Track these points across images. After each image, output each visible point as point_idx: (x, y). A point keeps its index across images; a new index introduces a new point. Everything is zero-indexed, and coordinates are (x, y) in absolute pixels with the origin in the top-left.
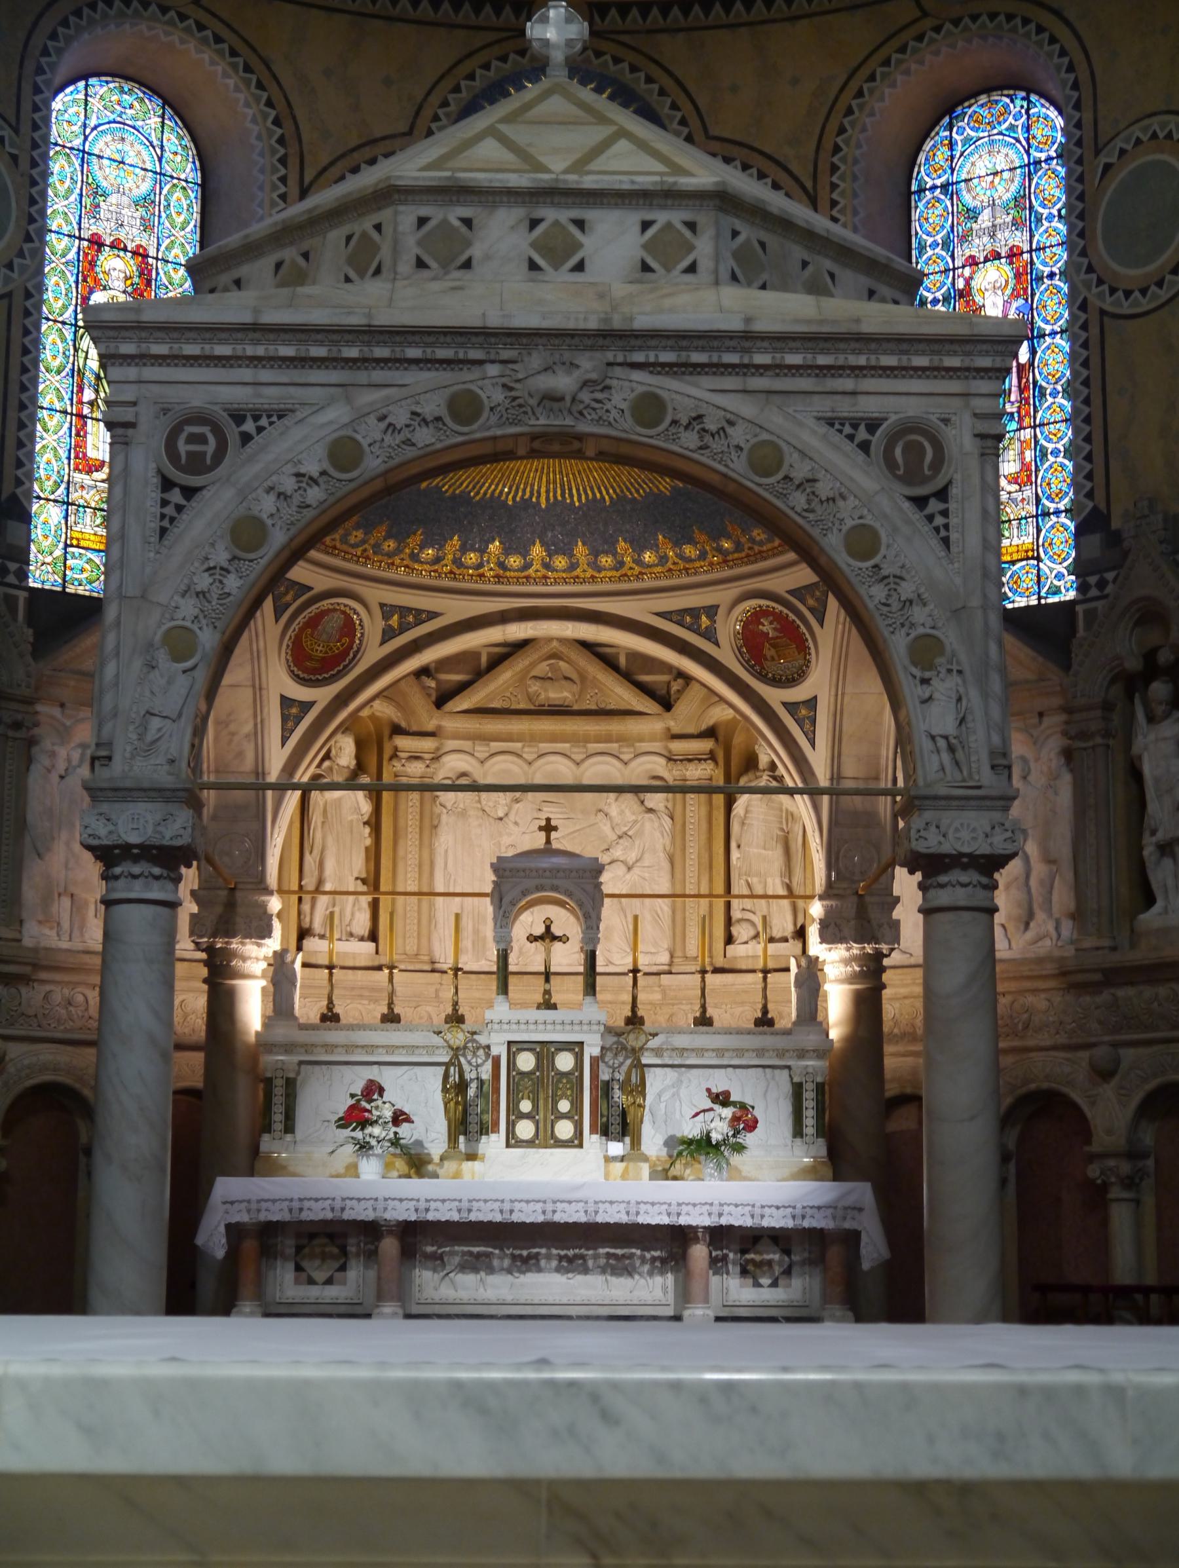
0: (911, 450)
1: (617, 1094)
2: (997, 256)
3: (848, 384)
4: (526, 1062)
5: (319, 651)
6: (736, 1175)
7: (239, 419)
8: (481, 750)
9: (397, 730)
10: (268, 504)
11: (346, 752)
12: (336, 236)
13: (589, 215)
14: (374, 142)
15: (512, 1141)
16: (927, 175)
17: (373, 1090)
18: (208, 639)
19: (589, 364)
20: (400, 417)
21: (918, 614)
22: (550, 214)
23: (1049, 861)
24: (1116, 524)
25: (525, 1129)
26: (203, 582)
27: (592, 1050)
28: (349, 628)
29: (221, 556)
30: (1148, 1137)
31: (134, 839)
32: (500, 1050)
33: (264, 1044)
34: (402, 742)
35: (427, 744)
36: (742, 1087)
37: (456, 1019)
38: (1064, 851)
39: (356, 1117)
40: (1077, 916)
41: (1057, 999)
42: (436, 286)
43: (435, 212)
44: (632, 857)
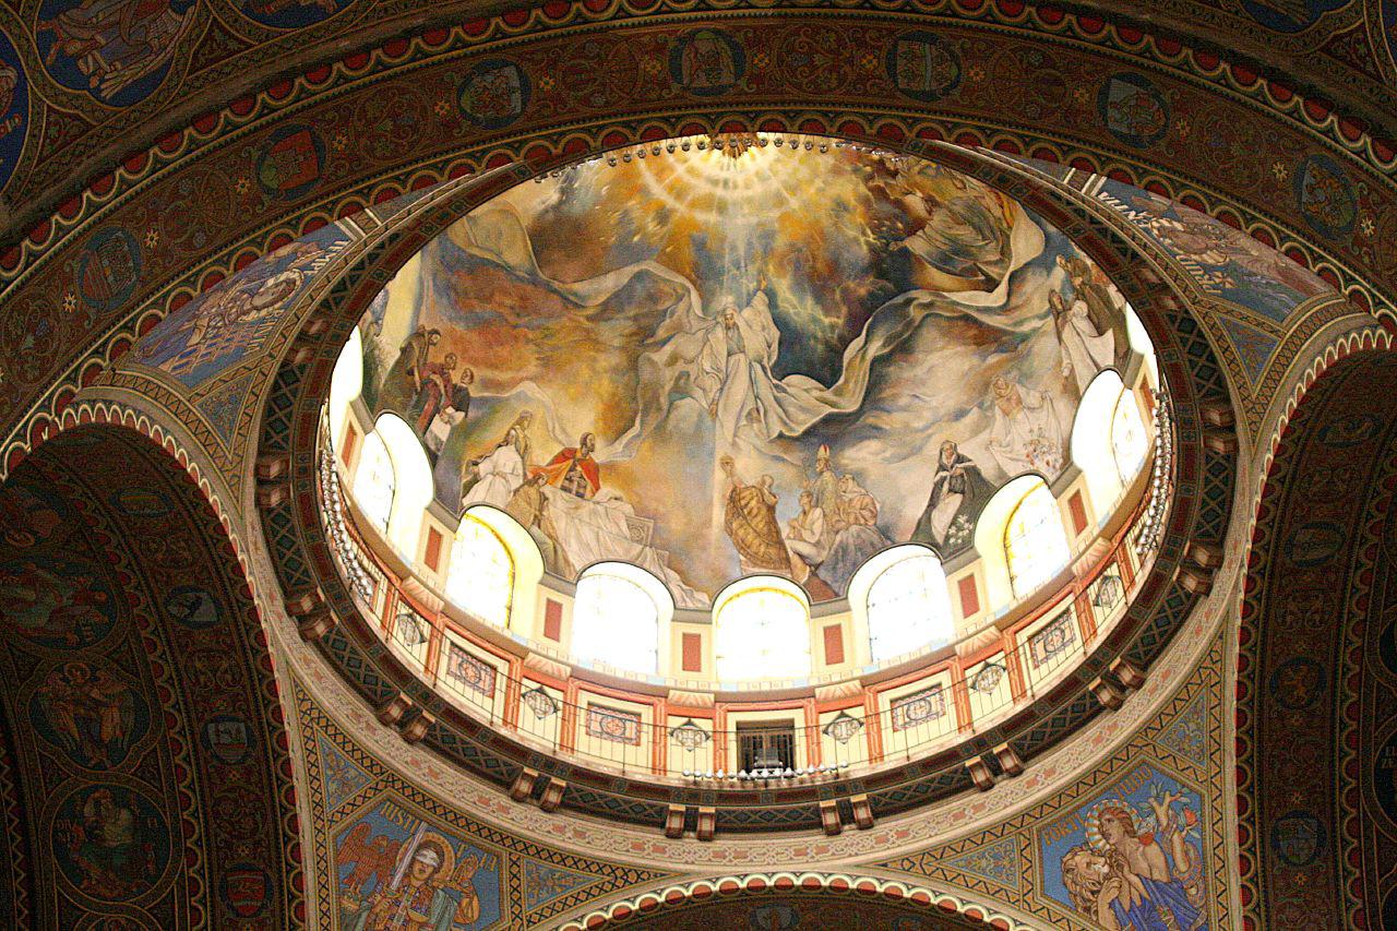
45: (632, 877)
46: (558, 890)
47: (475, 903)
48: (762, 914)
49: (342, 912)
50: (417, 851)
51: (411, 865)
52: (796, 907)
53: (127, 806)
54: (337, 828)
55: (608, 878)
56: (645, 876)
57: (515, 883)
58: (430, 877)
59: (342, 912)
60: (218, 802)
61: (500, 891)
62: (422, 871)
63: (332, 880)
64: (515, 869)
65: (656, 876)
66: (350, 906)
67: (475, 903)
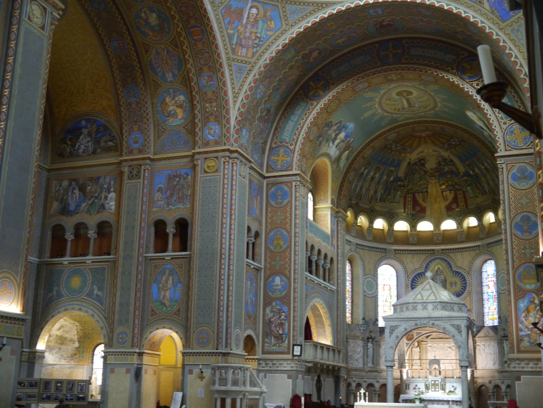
0: (458, 327)
1: (444, 386)
2: (491, 281)
3: (451, 321)
4: (433, 382)
5: (409, 337)
6: (456, 394)
7: (396, 326)
8: (432, 343)
9: (422, 341)
10: (399, 334)
11: (416, 344)
12: (405, 306)
13: (428, 304)
14: (416, 269)
15: (432, 391)
16: (483, 270)
17: (416, 386)
18: (394, 347)
19: (427, 320)
20: (410, 326)
21: (459, 343)
22: (424, 304)
23: (497, 357)
24: (502, 318)
25: (433, 390)
26: (394, 342)
27: (440, 381)
28: (413, 335)
29: (395, 339)
30: (508, 390)
31: (389, 365)
32: (430, 381)
33: (406, 380)
34: (423, 343)
35: (426, 343)
36: (455, 385)
37: (426, 377)
38: (498, 356)
39: (415, 388)
40: (499, 364)
41: (498, 374)
42: (414, 312)
43: (413, 304)
44: (451, 355)
45: (324, 6)
46: (300, 14)
47: (273, 22)
48: (371, 11)
49: (229, 35)
50: (250, 9)
51: (248, 15)
52: (382, 8)
53: (154, 12)
54: (221, 8)
55: (316, 7)
56: (328, 5)
57: (285, 14)
58: (256, 17)
59: (229, 35)
60: (181, 7)
61: (280, 17)
62: (252, 16)
63: (223, 25)
64: (284, 9)
65: (332, 4)
66: (231, 32)
67: (273, 22)
